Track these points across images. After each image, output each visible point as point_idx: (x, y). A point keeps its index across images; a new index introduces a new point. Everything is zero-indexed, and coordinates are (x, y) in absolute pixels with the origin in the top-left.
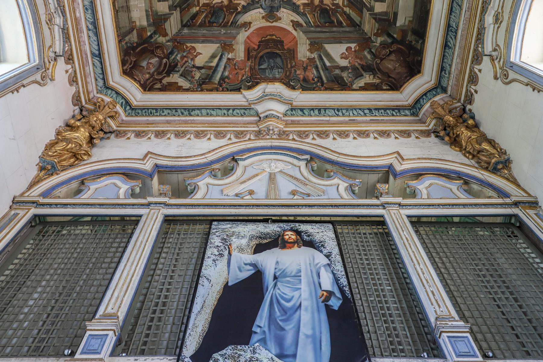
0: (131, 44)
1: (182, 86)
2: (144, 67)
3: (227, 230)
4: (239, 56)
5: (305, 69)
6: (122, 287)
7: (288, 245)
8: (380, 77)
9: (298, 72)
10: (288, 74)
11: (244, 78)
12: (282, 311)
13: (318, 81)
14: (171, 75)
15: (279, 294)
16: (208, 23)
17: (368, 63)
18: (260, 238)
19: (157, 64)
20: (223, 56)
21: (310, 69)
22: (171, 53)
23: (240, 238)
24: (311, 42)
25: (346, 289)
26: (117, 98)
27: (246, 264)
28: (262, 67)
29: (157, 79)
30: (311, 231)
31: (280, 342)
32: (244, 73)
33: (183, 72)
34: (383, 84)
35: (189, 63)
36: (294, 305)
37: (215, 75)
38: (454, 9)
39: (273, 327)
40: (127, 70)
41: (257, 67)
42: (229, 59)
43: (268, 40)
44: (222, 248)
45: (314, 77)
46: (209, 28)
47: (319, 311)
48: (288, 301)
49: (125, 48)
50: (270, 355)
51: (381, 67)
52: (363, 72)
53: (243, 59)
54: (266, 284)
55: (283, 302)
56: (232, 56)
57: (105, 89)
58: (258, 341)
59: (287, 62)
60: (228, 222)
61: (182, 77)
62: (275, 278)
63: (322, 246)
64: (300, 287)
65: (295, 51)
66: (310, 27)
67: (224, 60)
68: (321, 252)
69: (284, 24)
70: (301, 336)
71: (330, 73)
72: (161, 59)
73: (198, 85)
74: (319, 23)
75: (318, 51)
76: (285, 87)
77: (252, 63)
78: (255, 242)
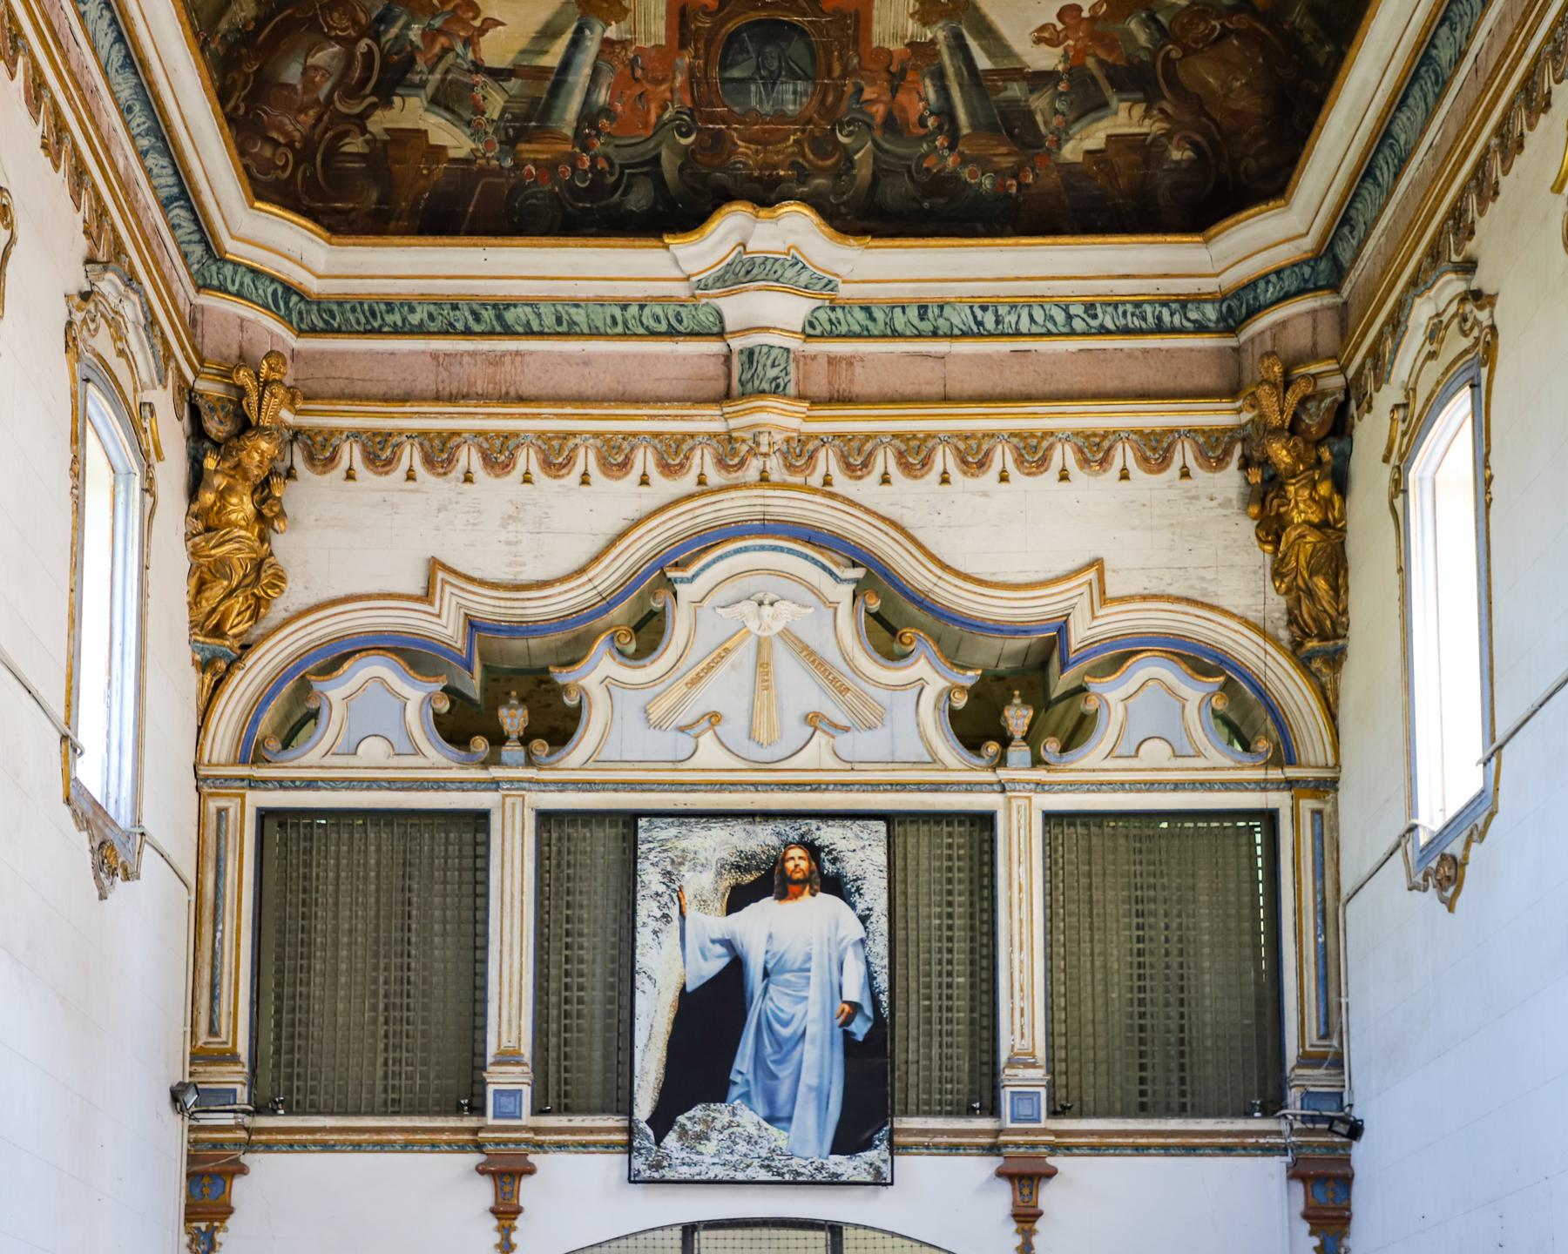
0: (239, 30)
1: (443, 148)
2: (292, 87)
3: (669, 845)
4: (647, 33)
5: (896, 81)
6: (510, 1001)
7: (792, 888)
8: (1170, 110)
9: (869, 94)
10: (830, 99)
11: (667, 116)
12: (776, 1046)
13: (940, 128)
14: (397, 100)
15: (772, 1011)
17: (1136, 61)
18: (738, 867)
19: (337, 66)
20: (587, 32)
21: (913, 82)
22: (386, 18)
23: (699, 868)
25: (884, 998)
26: (259, 284)
27: (713, 942)
28: (736, 73)
29: (347, 116)
30: (841, 845)
31: (770, 1098)
32: (668, 95)
33: (437, 89)
34: (1176, 139)
35: (458, 55)
36: (795, 1032)
37: (560, 103)
38: (1411, 101)
39: (760, 1073)
40: (236, 108)
41: (715, 73)
42: (607, 43)
44: (666, 898)
45: (927, 113)
47: (832, 1044)
48: (785, 1024)
49: (221, 53)
50: (757, 1118)
51: (1181, 74)
52: (1109, 92)
54: (749, 988)
55: (777, 1026)
56: (619, 31)
57: (211, 261)
58: (740, 1097)
59: (829, 53)
60: (670, 820)
61: (437, 110)
62: (766, 974)
63: (858, 889)
64: (804, 994)
67: (592, 46)
68: (853, 906)
70: (802, 1089)
72: (349, 43)
73: (500, 142)
77: (696, 57)
78: (729, 880)
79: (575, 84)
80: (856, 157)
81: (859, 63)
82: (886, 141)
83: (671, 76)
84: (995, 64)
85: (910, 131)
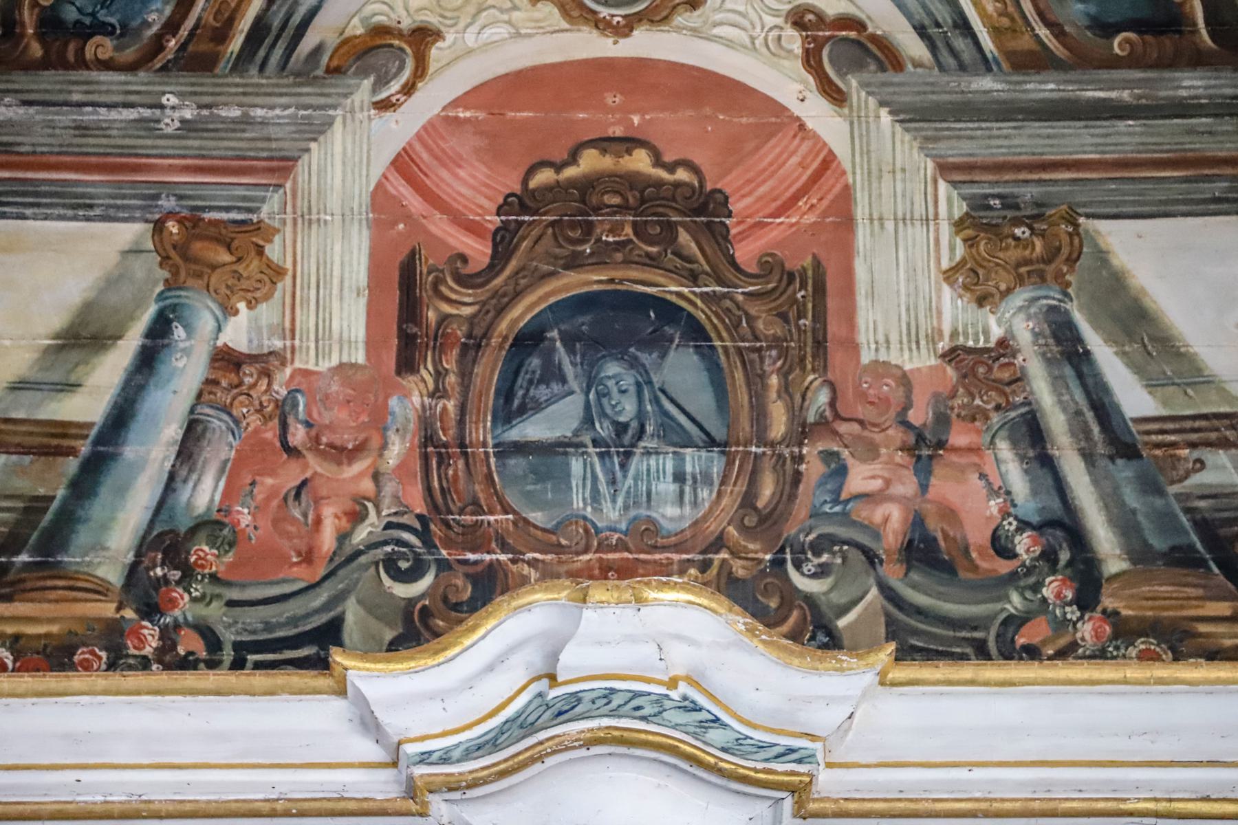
9: (861, 478)
10: (767, 490)
11: (361, 535)
13: (1049, 556)
16: (40, 36)
20: (179, 332)
24: (979, 204)
28: (532, 429)
32: (367, 486)
37: (97, 509)
41: (483, 432)
43: (587, 185)
45: (1011, 525)
46: (48, 81)
53: (360, 357)
56: (255, 327)
59: (756, 381)
65: (831, 285)
66: (962, 67)
69: (729, 43)
71: (1151, 486)
74: (1043, 32)
75: (1042, 278)
76: (741, 621)
77: (438, 393)
79: (138, 467)
80: (842, 623)
81: (832, 404)
82: (914, 586)
83: (375, 442)
84: (1165, 403)
85: (975, 568)
